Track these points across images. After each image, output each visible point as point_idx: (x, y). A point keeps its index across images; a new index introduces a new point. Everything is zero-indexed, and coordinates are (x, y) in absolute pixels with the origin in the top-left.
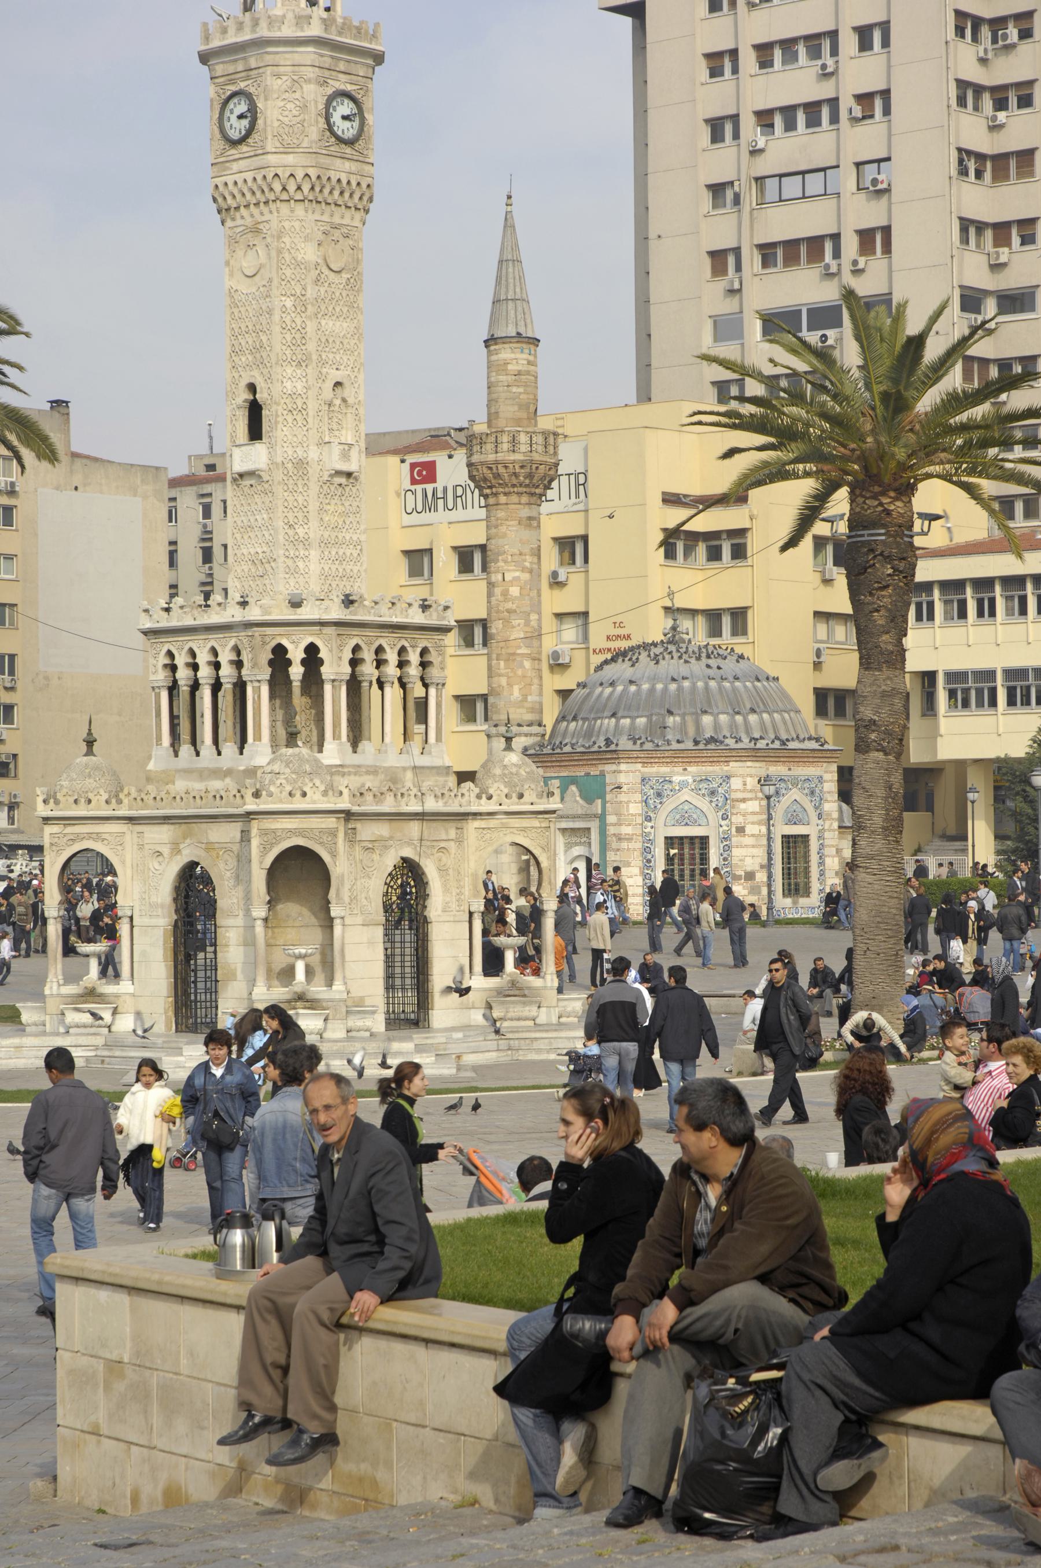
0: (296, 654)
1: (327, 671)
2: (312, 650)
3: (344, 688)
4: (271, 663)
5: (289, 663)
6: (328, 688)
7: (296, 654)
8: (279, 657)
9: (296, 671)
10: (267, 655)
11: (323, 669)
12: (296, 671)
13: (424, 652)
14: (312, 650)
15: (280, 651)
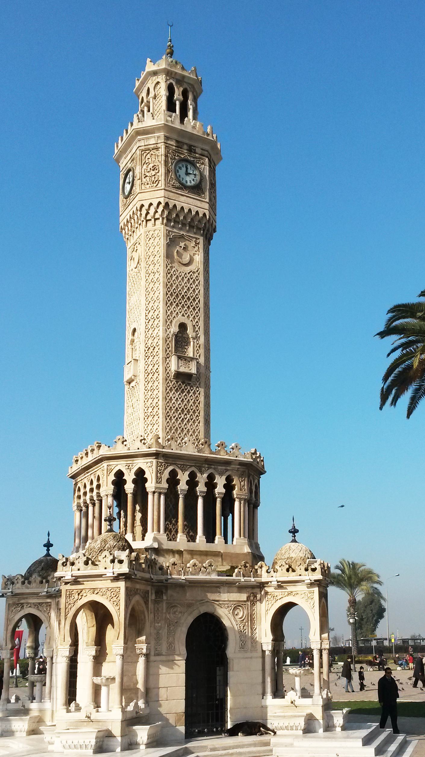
0: (129, 477)
1: (150, 486)
2: (140, 473)
3: (162, 497)
4: (114, 483)
5: (125, 482)
6: (150, 497)
7: (129, 477)
8: (119, 480)
9: (129, 487)
10: (112, 477)
11: (147, 485)
12: (129, 487)
13: (229, 480)
14: (140, 473)
15: (120, 474)
